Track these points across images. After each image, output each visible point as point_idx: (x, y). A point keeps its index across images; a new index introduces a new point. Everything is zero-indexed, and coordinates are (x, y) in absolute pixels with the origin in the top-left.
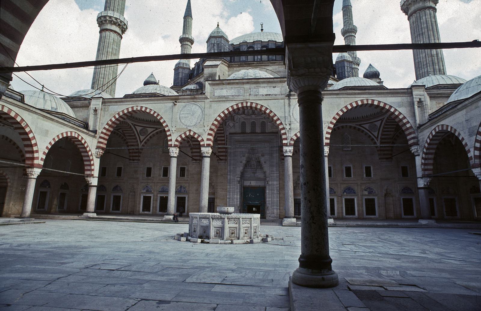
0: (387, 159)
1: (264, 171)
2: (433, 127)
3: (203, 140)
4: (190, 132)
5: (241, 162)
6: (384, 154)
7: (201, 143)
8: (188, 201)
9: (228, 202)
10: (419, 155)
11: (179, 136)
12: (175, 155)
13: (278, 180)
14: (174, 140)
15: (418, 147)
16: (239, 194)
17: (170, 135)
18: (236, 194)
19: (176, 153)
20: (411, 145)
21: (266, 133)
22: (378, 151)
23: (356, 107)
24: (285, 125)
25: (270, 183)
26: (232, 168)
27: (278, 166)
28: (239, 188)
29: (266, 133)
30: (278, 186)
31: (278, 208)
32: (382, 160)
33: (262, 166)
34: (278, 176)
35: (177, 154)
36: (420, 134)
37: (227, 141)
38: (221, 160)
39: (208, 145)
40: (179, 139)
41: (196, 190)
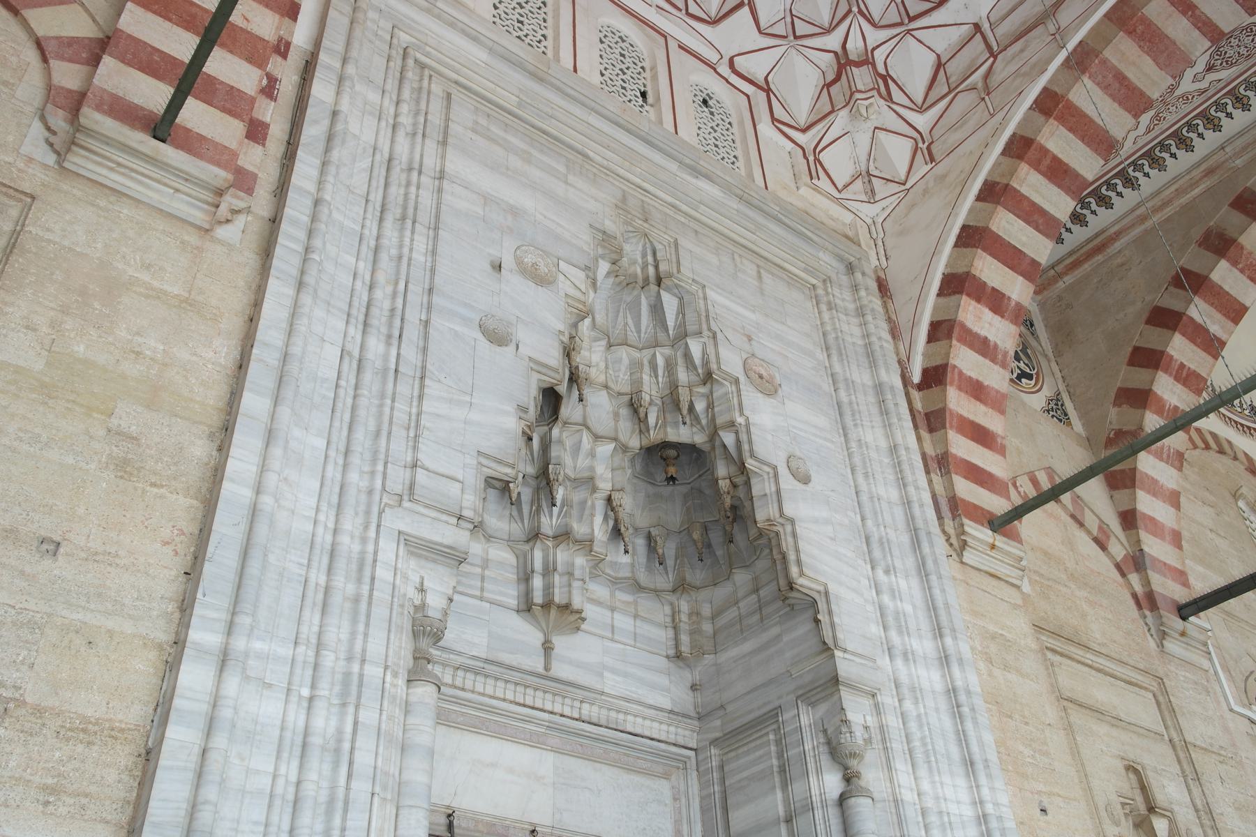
5: (498, 337)
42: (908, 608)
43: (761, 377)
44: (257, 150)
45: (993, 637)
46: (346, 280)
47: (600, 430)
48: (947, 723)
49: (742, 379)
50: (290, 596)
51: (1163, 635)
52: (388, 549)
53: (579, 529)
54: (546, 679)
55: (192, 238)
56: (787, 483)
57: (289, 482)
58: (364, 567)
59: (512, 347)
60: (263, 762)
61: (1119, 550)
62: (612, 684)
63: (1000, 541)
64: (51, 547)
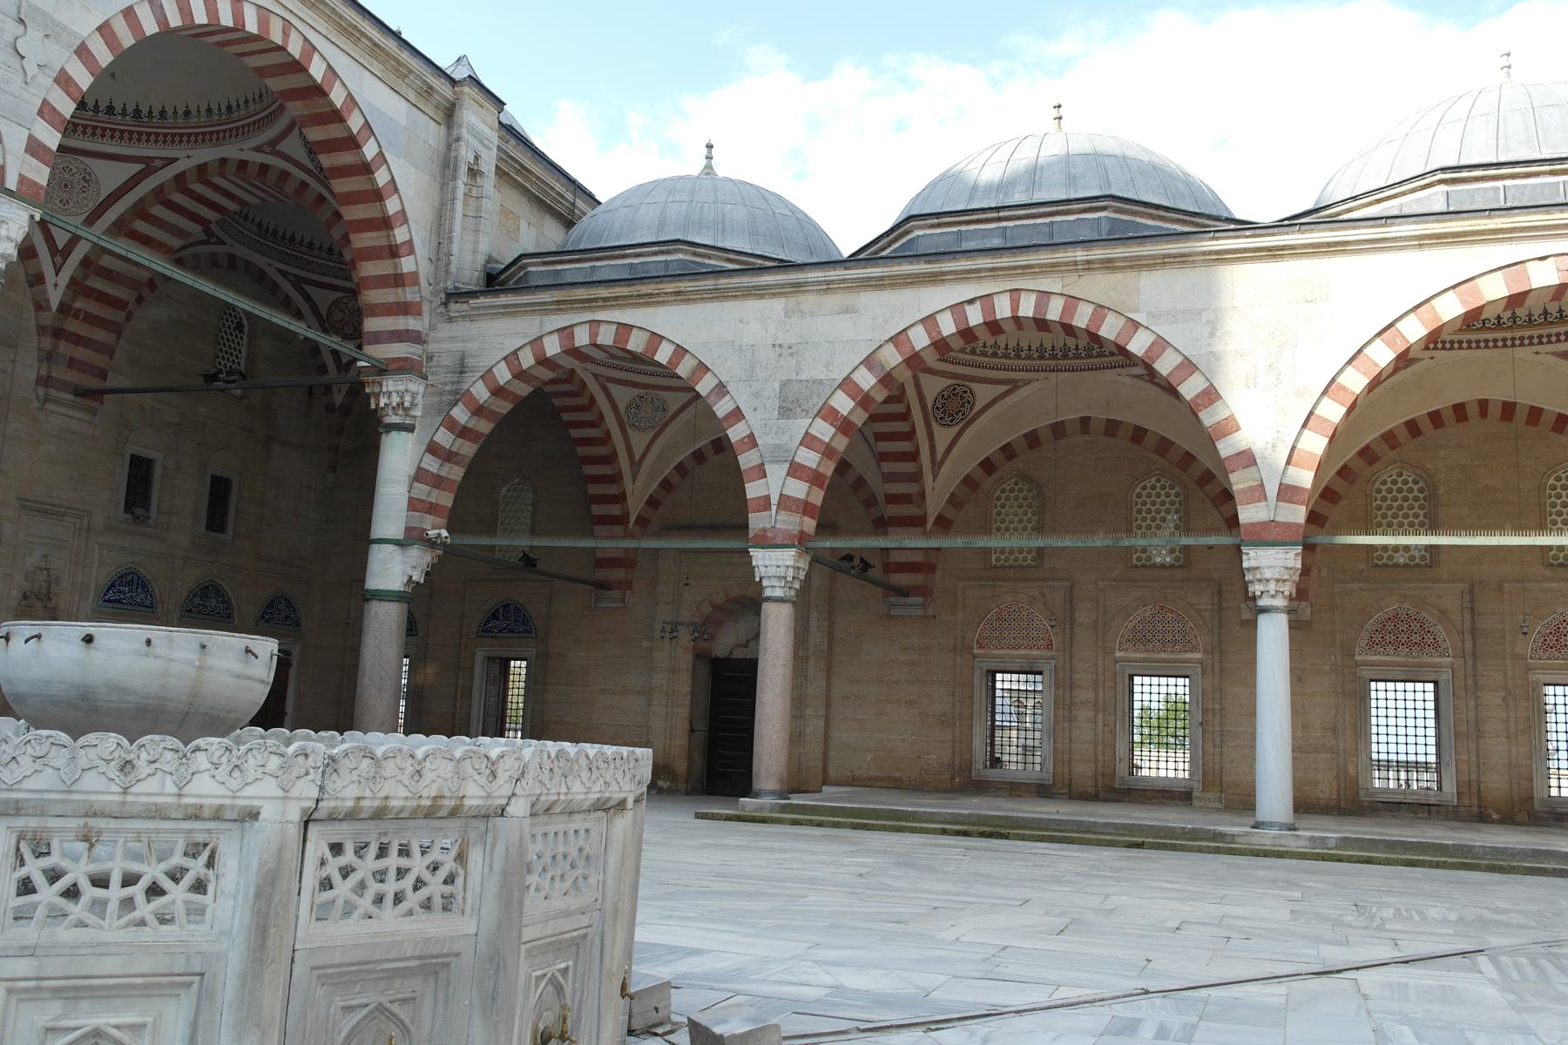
0: (80, 392)
2: (562, 320)
6: (72, 363)
10: (410, 429)
15: (422, 389)
20: (381, 369)
22: (42, 330)
23: (228, 30)
32: (52, 392)
36: (445, 330)
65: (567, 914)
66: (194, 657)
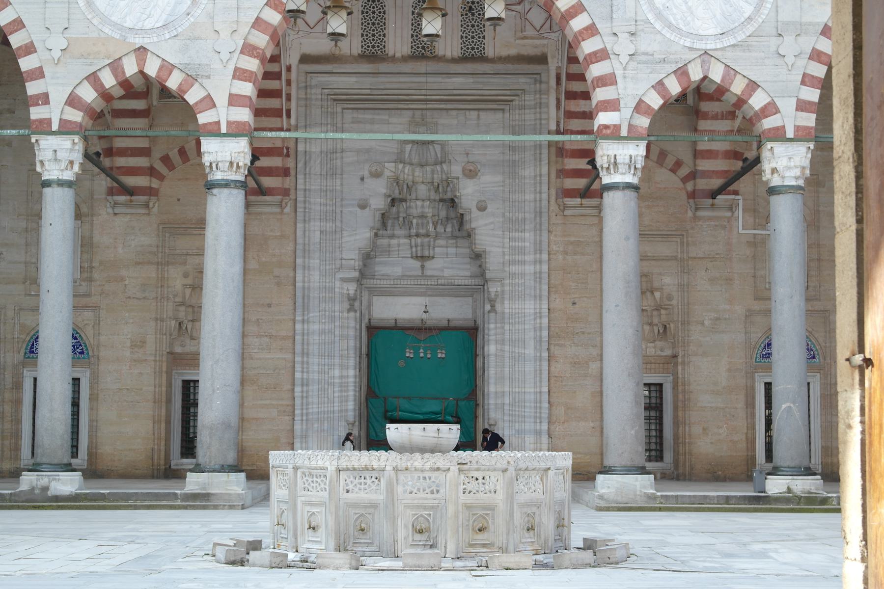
1: (478, 248)
3: (209, 102)
4: (141, 61)
5: (363, 206)
7: (203, 118)
8: (93, 398)
9: (298, 402)
11: (87, 78)
12: (68, 176)
13: (545, 293)
14: (58, 97)
16: (352, 362)
17: (39, 73)
18: (337, 361)
19: (71, 163)
21: (483, 59)
24: (609, 43)
25: (506, 307)
26: (316, 237)
27: (545, 226)
28: (352, 333)
29: (483, 59)
30: (545, 321)
31: (545, 427)
33: (467, 227)
34: (545, 276)
35: (76, 168)
37: (289, 98)
38: (262, 191)
39: (236, 131)
40: (88, 94)
41: (133, 346)
42: (527, 244)
43: (470, 171)
44: (288, 179)
45: (572, 243)
46: (318, 208)
47: (424, 198)
48: (532, 282)
49: (461, 176)
50: (317, 302)
51: (697, 209)
52: (338, 284)
53: (422, 231)
54: (423, 276)
55: (279, 217)
56: (475, 213)
57: (313, 276)
58: (332, 289)
59: (368, 209)
60: (316, 337)
61: (684, 171)
62: (447, 273)
63: (585, 201)
64: (270, 305)
65: (426, 499)
66: (407, 431)
